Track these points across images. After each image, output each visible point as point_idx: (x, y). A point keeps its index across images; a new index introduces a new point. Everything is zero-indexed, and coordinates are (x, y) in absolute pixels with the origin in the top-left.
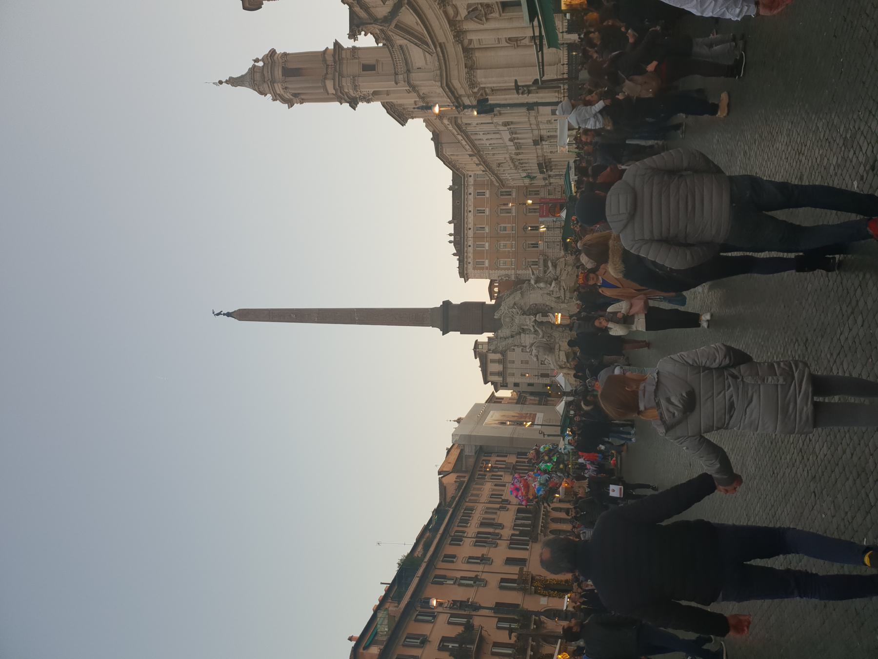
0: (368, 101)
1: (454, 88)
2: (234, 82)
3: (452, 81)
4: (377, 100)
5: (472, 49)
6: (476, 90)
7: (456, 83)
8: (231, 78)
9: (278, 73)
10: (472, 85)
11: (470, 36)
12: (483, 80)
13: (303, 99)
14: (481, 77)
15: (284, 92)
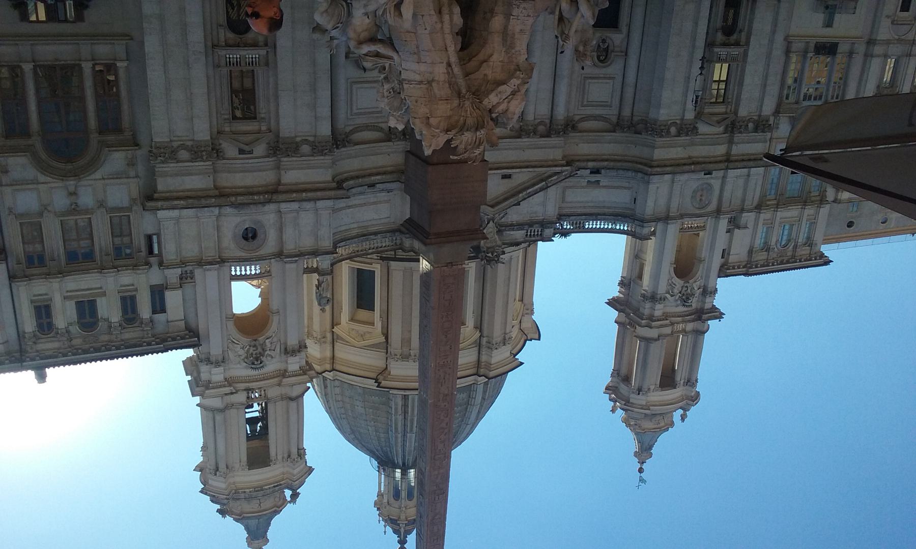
0: (709, 292)
1: (682, 159)
2: (644, 452)
3: (655, 158)
4: (708, 277)
5: (618, 119)
6: (703, 128)
7: (660, 154)
8: (636, 454)
9: (623, 388)
10: (686, 129)
11: (561, 113)
12: (662, 111)
13: (688, 381)
14: (664, 114)
15: (643, 394)
